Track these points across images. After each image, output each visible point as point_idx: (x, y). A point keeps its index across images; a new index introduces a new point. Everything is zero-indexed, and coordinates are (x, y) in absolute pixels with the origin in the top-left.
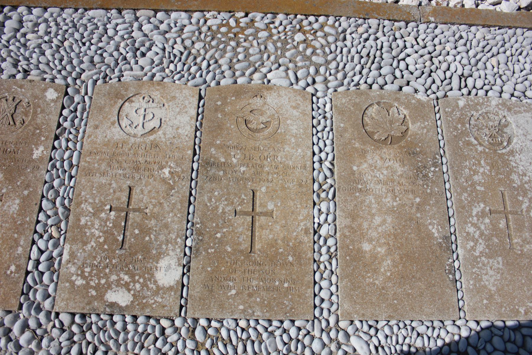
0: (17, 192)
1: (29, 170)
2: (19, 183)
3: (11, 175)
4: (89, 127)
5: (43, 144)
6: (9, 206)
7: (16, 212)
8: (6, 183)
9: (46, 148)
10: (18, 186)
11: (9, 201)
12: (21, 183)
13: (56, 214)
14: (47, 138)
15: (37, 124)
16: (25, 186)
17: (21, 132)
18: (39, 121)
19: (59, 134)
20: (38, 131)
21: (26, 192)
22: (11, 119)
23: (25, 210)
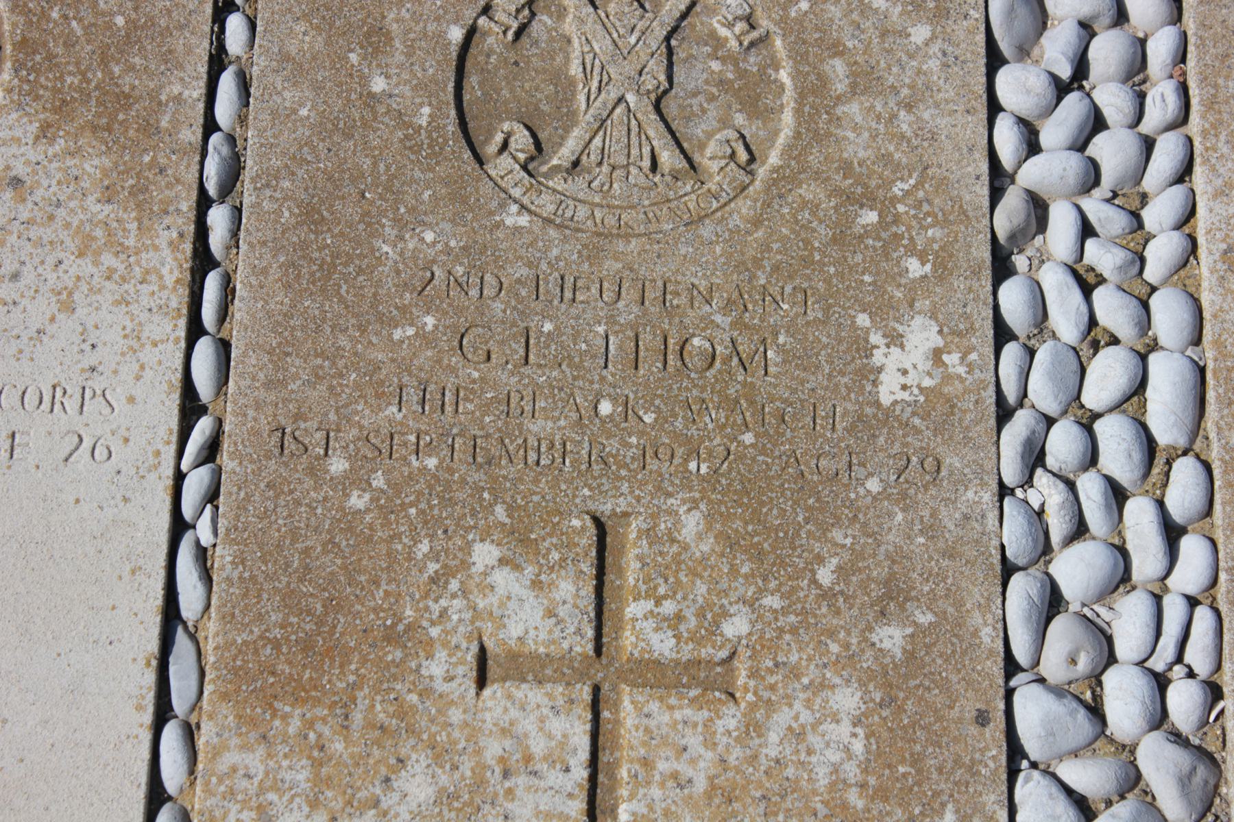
0: (832, 633)
1: (873, 485)
2: (825, 576)
3: (757, 518)
4: (1218, 194)
5: (923, 304)
6: (797, 734)
7: (851, 771)
8: (734, 571)
9: (954, 334)
10: (827, 595)
11: (789, 700)
12: (839, 569)
13: (1132, 781)
14: (943, 266)
15: (846, 168)
16: (876, 591)
17: (757, 223)
18: (857, 148)
19: (1012, 237)
20: (870, 217)
21: (891, 638)
22: (654, 129)
23: (916, 760)
